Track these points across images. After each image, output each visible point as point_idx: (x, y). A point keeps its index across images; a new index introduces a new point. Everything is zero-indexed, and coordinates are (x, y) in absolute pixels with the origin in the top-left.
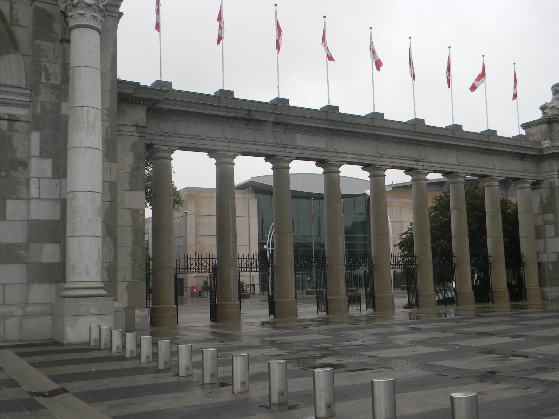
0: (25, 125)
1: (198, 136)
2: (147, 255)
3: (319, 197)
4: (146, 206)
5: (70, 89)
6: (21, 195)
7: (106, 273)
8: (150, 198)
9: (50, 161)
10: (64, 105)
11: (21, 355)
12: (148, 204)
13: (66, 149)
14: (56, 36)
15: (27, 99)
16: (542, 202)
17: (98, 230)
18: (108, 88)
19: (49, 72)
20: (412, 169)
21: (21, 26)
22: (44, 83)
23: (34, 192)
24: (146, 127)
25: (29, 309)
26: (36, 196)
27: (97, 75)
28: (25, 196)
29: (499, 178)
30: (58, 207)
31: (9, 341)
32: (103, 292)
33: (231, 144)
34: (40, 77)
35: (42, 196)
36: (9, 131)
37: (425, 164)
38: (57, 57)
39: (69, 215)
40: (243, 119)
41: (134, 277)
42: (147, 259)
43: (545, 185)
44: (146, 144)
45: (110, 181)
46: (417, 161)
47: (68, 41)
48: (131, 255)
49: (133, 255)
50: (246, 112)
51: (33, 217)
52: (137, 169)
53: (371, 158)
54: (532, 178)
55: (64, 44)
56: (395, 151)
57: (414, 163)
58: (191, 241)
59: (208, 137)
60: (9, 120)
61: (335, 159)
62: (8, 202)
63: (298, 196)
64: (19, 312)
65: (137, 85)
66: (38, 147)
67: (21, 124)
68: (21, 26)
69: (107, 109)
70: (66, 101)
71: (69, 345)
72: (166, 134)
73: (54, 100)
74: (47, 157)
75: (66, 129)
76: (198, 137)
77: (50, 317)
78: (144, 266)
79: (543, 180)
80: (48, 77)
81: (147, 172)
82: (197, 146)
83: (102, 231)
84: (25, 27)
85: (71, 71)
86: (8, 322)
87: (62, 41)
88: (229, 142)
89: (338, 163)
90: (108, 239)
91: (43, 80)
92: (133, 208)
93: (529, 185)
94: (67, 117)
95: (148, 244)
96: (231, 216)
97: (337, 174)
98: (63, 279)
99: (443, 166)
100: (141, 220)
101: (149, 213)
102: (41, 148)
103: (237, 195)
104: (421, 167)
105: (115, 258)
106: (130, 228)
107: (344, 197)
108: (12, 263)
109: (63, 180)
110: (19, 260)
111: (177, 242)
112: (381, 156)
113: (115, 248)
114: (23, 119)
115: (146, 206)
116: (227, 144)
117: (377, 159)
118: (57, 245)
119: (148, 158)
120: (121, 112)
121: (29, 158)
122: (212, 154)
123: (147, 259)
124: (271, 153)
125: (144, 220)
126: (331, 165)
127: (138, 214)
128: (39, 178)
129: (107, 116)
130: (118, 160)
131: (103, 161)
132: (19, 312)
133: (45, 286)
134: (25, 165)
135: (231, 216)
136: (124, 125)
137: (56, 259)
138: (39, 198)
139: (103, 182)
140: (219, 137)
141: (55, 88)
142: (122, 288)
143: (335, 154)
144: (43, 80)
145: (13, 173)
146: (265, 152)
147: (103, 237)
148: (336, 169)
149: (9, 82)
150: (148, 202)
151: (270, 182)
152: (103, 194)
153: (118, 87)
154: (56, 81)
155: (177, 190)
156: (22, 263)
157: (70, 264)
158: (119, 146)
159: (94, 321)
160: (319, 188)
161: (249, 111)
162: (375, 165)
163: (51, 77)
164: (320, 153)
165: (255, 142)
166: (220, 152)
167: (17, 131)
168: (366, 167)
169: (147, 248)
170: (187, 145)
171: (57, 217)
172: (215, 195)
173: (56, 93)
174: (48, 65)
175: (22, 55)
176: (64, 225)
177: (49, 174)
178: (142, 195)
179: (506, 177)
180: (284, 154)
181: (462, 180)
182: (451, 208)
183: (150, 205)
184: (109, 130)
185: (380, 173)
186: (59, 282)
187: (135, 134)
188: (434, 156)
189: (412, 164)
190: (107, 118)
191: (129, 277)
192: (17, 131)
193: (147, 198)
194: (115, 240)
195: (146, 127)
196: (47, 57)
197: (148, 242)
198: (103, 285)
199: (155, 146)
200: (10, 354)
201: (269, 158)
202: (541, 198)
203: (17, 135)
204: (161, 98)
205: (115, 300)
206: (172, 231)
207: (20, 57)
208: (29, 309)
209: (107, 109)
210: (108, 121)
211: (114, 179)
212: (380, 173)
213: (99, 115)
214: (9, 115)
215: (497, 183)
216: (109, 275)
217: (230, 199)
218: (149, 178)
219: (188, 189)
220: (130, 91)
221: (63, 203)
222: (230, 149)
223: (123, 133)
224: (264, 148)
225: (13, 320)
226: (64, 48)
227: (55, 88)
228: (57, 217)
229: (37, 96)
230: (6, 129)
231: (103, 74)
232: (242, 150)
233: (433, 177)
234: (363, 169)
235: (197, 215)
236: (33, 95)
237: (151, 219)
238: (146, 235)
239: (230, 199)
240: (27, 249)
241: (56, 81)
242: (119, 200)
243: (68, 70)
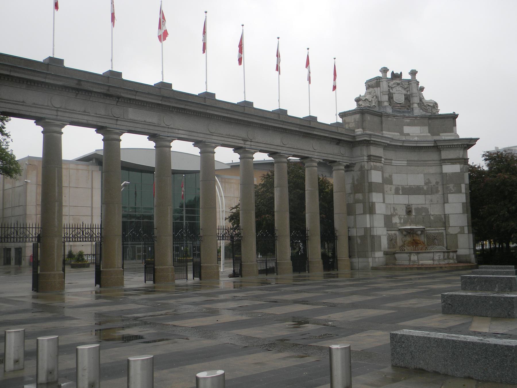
1: (23, 102)
3: (149, 170)
16: (353, 183)
20: (241, 148)
29: (317, 160)
33: (60, 113)
37: (252, 143)
40: (73, 89)
43: (356, 168)
46: (245, 140)
50: (76, 82)
53: (201, 135)
54: (346, 161)
56: (226, 130)
57: (242, 142)
59: (34, 104)
61: (166, 134)
63: (128, 167)
79: (355, 164)
82: (21, 112)
88: (57, 111)
89: (169, 139)
93: (343, 168)
96: (56, 185)
97: (168, 149)
99: (268, 146)
104: (249, 146)
107: (175, 172)
112: (212, 134)
116: (55, 113)
117: (208, 136)
122: (39, 121)
135: (56, 185)
140: (46, 104)
143: (166, 130)
146: (95, 123)
148: (167, 144)
151: (102, 153)
160: (151, 162)
161: (80, 81)
162: (205, 142)
164: (151, 127)
165: (85, 113)
166: (47, 120)
168: (197, 143)
179: (324, 160)
180: (115, 126)
181: (285, 160)
182: (275, 186)
185: (210, 149)
188: (261, 137)
189: (241, 143)
201: (100, 129)
202: (353, 179)
212: (210, 149)
215: (316, 164)
217: (56, 168)
222: (59, 117)
224: (95, 119)
232: (71, 119)
233: (260, 157)
234: (195, 145)
239: (56, 168)
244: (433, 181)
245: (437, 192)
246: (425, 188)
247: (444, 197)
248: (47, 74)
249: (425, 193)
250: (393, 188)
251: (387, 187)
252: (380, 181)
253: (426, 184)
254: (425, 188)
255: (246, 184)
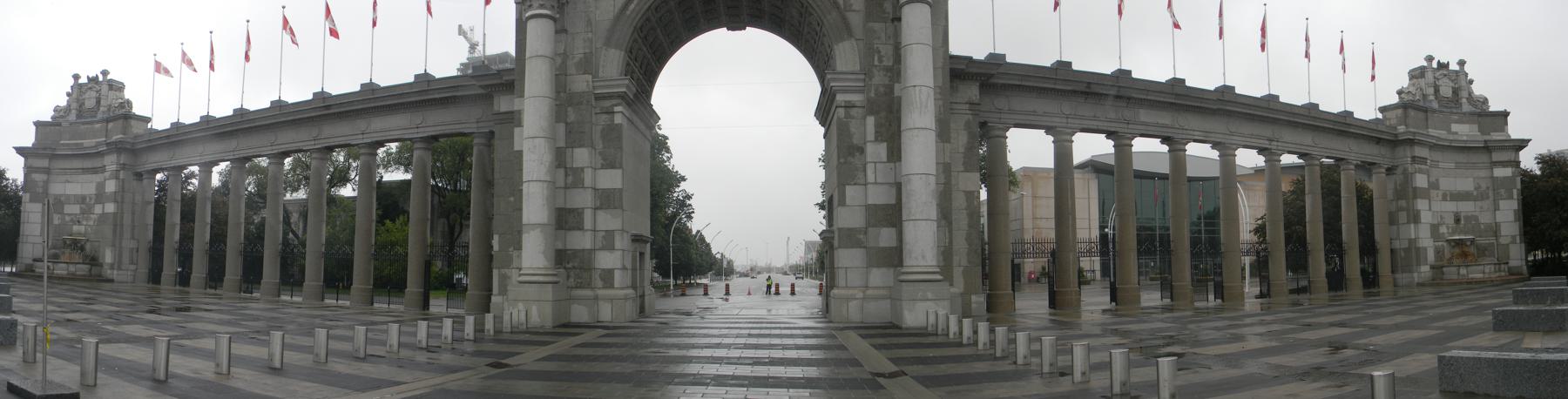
0: (860, 110)
1: (1034, 112)
2: (983, 239)
3: (1163, 177)
4: (981, 188)
5: (902, 70)
6: (859, 181)
7: (941, 258)
8: (985, 179)
9: (885, 144)
10: (897, 86)
11: (863, 337)
12: (983, 186)
13: (899, 132)
14: (886, 15)
15: (862, 84)
16: (1396, 189)
17: (933, 213)
18: (940, 64)
19: (882, 54)
20: (1266, 149)
21: (854, 11)
22: (876, 66)
23: (871, 177)
24: (979, 104)
25: (869, 292)
26: (873, 181)
27: (929, 52)
28: (862, 181)
29: (1355, 162)
30: (894, 191)
31: (852, 323)
32: (938, 277)
34: (873, 59)
35: (879, 181)
36: (845, 118)
37: (1279, 144)
38: (889, 37)
39: (904, 200)
41: (969, 262)
42: (983, 243)
43: (1399, 171)
44: (980, 123)
45: (944, 163)
46: (1271, 140)
47: (899, 19)
48: (966, 240)
49: (968, 239)
50: (1085, 85)
51: (870, 202)
52: (971, 149)
53: (1221, 136)
54: (1386, 163)
55: (896, 23)
56: (1247, 128)
57: (1267, 142)
58: (1028, 224)
60: (845, 107)
61: (1180, 136)
62: (847, 187)
63: (1141, 176)
64: (860, 295)
65: (970, 59)
66: (874, 132)
67: (855, 110)
68: (854, 11)
69: (940, 88)
70: (899, 81)
71: (907, 329)
72: (1000, 111)
73: (887, 82)
74: (882, 141)
75: (899, 111)
76: (1034, 113)
77: (889, 301)
78: (980, 251)
79: (1397, 166)
80: (880, 60)
81: (981, 152)
82: (1033, 123)
83: (937, 215)
84: (858, 11)
85: (903, 50)
86: (850, 304)
87: (893, 20)
89: (1184, 141)
90: (943, 222)
91: (876, 63)
92: (968, 190)
93: (1384, 170)
94: (900, 98)
95: (983, 227)
97: (1182, 153)
98: (900, 263)
99: (1299, 147)
100: (975, 203)
101: (984, 195)
102: (876, 132)
103: (1076, 176)
104: (1275, 147)
105: (951, 242)
106: (965, 211)
107: (1191, 180)
108: (852, 247)
109: (897, 164)
110: (858, 244)
111: (1014, 226)
112: (1232, 134)
113: (950, 232)
114: (858, 104)
115: (981, 188)
117: (1227, 137)
118: (894, 229)
119: (982, 137)
120: (953, 89)
121: (865, 143)
122: (1049, 130)
123: (983, 243)
124: (1113, 129)
125: (979, 203)
126: (1177, 142)
127: (972, 196)
128: (875, 163)
129: (940, 94)
130: (952, 141)
131: (937, 142)
132: (860, 295)
133: (884, 270)
134: (862, 150)
136: (956, 103)
137: (894, 244)
138: (876, 183)
139: (937, 163)
141: (888, 69)
142: (958, 273)
143: (1180, 131)
144: (876, 63)
145: (850, 159)
146: (1105, 128)
147: (938, 221)
148: (1182, 147)
149: (844, 70)
150: (983, 183)
151: (1112, 161)
152: (937, 176)
153: (951, 63)
154: (888, 62)
155: (1014, 170)
156: (861, 247)
157: (906, 248)
158: (952, 125)
159: (931, 307)
160: (1164, 168)
162: (1224, 143)
163: (884, 59)
164: (1164, 130)
165: (1095, 118)
167: (853, 118)
168: (1215, 146)
169: (983, 232)
170: (1023, 122)
171: (893, 202)
172: (1052, 175)
173: (889, 74)
174: (881, 47)
175: (857, 40)
176: (900, 210)
177: (885, 160)
178: (977, 176)
179: (1362, 162)
180: (1126, 131)
181: (1317, 162)
182: (1306, 192)
183: (985, 186)
184: (942, 109)
185: (1231, 152)
186: (896, 266)
187: (968, 112)
188: (1288, 136)
189: (1265, 144)
190: (939, 96)
191: (964, 262)
192: (853, 118)
193: (981, 180)
194: (950, 224)
195: (979, 104)
196: (879, 38)
197: (983, 225)
198: (938, 270)
199: (990, 124)
200: (853, 335)
201: (1110, 135)
202: (1396, 183)
203: (853, 121)
204: (993, 72)
205: (951, 285)
206: (1008, 214)
207: (855, 43)
208: (869, 292)
209: (940, 88)
210: (941, 99)
211: (948, 160)
212: (1231, 152)
213: (932, 94)
214: (846, 102)
215: (1352, 167)
216: (944, 260)
218: (984, 158)
219: (1025, 169)
220: (963, 67)
221: (899, 187)
223: (955, 111)
224: (1106, 124)
225: (855, 302)
226: (896, 26)
227: (888, 69)
228: (893, 202)
229: (871, 80)
230: (843, 116)
231: (934, 49)
233: (1288, 159)
234: (1213, 148)
235: (1035, 197)
236: (867, 79)
237: (986, 202)
238: (982, 219)
240: (866, 233)
241: (888, 62)
242: (953, 182)
243: (900, 49)
244: (1484, 186)
245: (1488, 198)
246: (1475, 193)
247: (1495, 204)
248: (1056, 79)
249: (1475, 200)
250: (1440, 193)
251: (1433, 193)
252: (1426, 186)
253: (1476, 189)
254: (1475, 193)
255: (1272, 191)
